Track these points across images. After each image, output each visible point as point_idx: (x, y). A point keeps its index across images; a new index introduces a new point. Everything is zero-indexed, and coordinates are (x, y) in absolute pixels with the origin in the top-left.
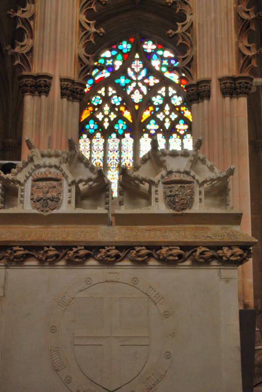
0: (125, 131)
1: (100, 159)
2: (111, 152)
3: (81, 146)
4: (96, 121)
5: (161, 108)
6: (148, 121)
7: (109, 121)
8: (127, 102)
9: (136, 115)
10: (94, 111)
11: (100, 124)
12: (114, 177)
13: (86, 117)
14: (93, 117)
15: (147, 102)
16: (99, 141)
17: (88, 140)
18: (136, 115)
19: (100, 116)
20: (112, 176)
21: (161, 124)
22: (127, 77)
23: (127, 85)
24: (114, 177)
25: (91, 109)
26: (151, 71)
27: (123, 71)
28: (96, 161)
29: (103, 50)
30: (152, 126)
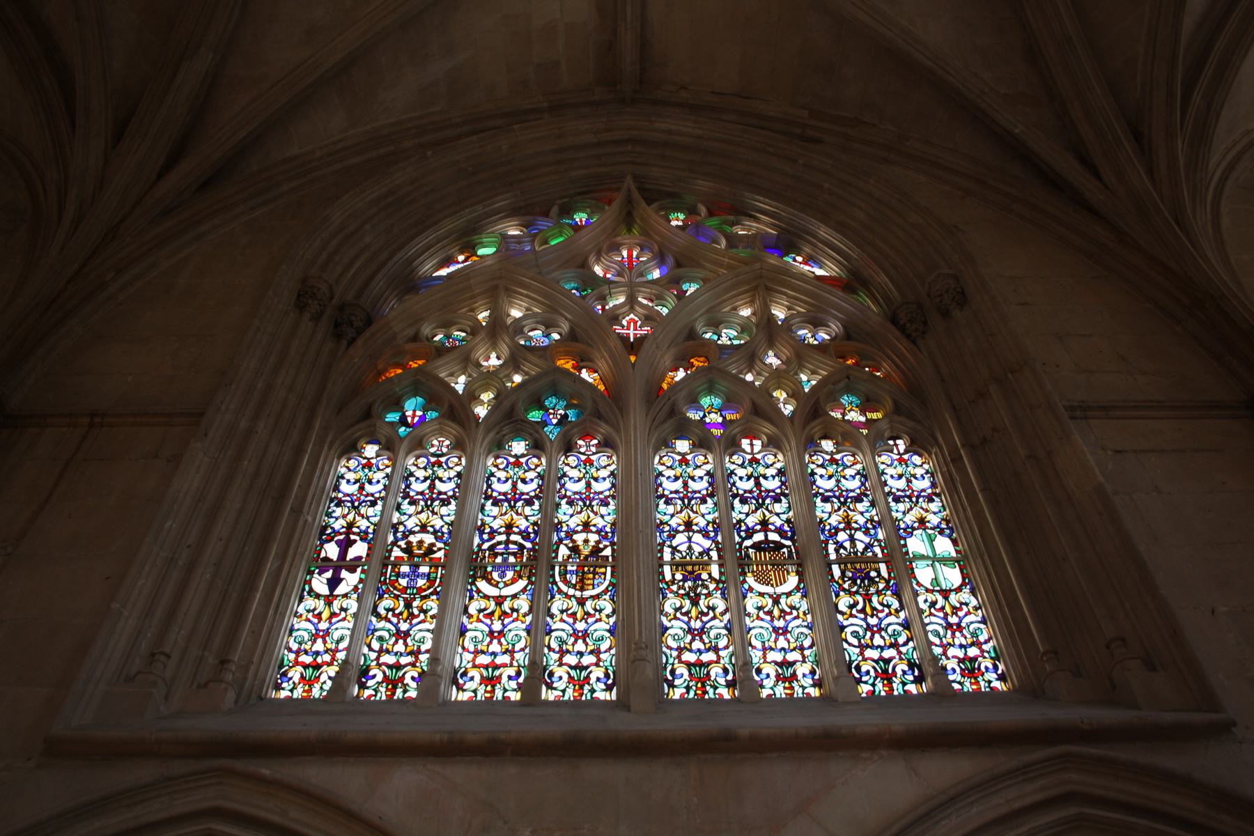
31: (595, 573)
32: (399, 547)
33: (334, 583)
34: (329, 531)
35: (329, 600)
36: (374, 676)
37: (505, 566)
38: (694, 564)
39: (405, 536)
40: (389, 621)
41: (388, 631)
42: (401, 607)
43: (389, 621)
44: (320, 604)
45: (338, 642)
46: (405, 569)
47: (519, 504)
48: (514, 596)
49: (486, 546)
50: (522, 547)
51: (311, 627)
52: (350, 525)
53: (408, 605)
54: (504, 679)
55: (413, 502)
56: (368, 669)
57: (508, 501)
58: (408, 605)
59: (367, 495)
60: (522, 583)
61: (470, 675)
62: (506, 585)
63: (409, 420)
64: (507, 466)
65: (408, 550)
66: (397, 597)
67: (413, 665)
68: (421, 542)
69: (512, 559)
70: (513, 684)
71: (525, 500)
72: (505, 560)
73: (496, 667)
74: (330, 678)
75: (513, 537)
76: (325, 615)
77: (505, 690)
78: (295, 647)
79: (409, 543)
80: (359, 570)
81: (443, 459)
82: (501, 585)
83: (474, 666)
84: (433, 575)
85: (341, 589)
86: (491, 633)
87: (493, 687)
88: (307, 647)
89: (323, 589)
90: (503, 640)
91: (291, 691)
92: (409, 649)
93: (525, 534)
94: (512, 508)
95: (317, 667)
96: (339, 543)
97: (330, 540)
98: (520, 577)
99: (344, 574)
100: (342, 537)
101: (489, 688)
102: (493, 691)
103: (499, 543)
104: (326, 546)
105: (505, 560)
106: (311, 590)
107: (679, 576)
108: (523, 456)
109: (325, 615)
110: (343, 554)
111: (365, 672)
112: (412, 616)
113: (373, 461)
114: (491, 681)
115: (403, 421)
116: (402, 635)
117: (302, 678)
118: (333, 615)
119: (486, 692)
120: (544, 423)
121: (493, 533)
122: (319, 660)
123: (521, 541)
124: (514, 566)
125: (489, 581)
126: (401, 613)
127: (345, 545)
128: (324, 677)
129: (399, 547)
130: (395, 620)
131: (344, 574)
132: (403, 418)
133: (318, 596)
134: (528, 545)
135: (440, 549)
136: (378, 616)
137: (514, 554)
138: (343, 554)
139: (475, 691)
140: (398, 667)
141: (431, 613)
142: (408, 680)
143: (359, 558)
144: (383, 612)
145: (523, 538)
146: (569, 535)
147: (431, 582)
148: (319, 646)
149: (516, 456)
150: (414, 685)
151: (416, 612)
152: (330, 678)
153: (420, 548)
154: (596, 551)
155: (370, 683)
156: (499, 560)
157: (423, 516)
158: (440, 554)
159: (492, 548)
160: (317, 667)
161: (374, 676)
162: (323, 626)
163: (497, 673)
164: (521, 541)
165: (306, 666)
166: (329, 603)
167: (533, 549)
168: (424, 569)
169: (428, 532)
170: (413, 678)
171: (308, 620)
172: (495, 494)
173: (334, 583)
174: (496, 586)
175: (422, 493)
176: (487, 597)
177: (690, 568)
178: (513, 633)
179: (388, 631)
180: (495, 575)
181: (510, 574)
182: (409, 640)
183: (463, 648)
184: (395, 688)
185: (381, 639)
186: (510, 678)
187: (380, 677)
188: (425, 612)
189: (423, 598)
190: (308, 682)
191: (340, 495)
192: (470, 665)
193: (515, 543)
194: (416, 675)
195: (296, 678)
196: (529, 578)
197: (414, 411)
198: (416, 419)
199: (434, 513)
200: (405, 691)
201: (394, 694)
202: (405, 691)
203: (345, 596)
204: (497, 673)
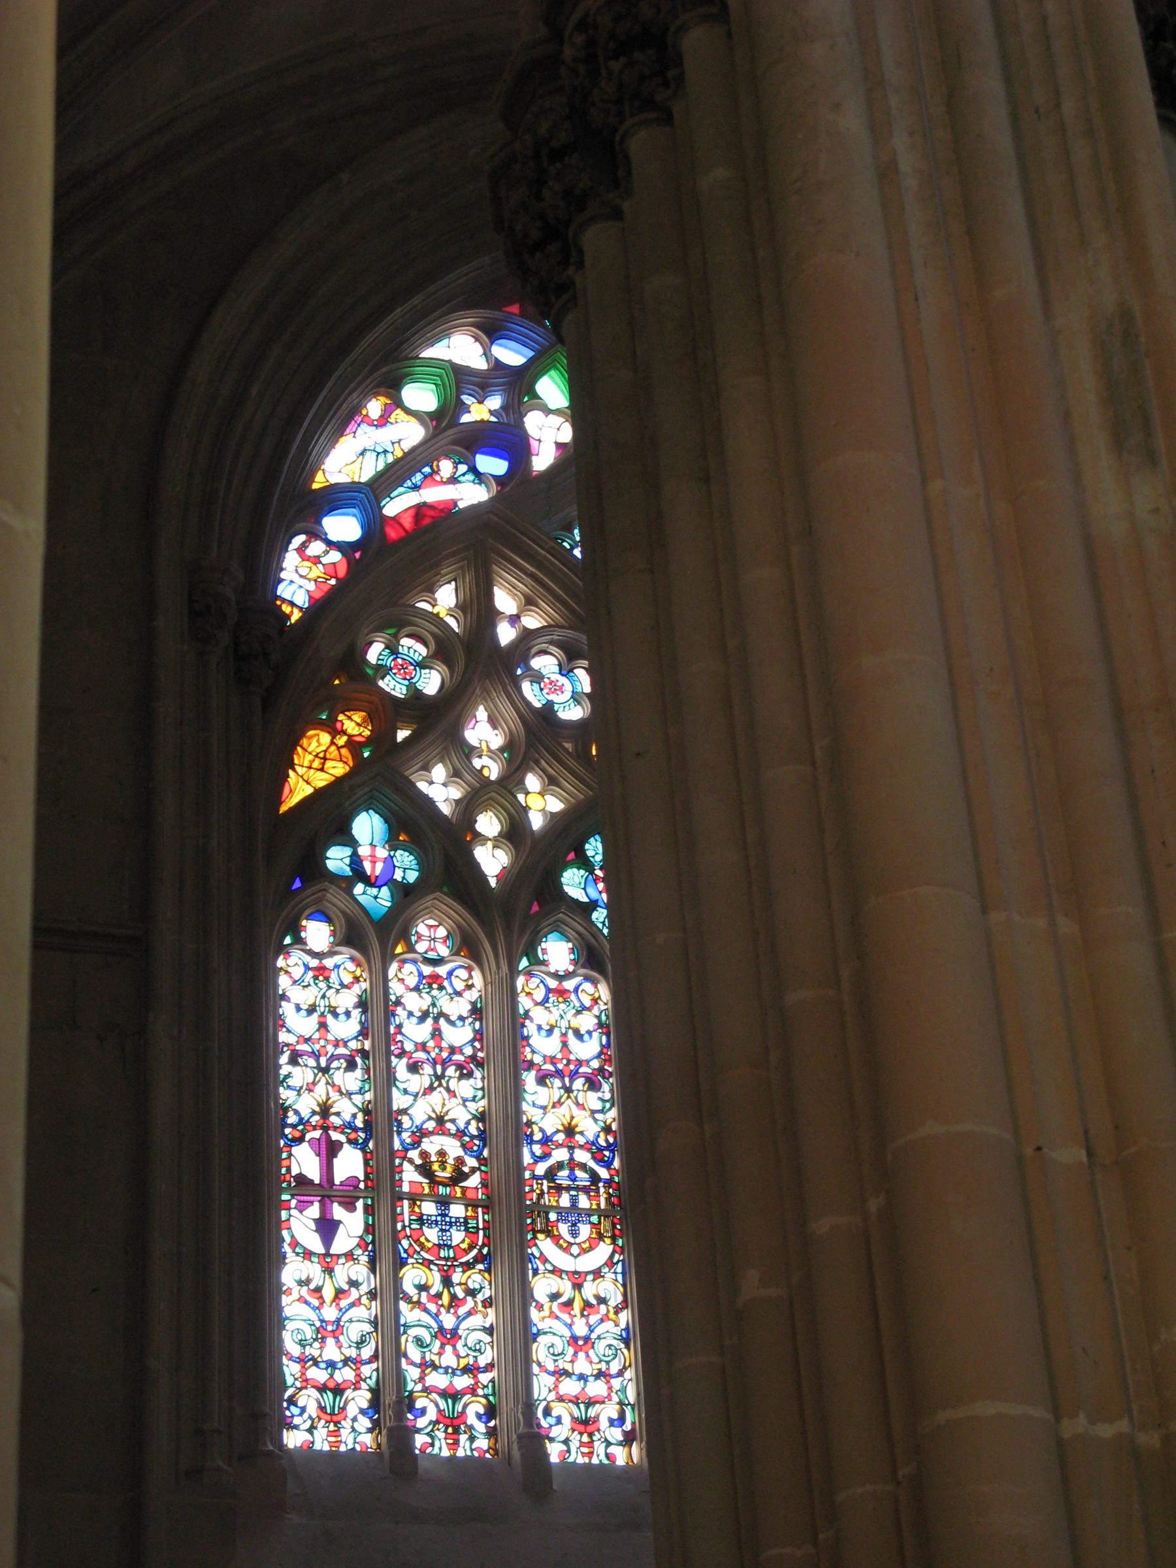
1: (460, 1134)
2: (542, 1080)
3: (287, 1009)
7: (515, 831)
10: (381, 738)
11: (441, 846)
12: (590, 1289)
13: (321, 780)
14: (378, 777)
16: (437, 992)
17: (344, 964)
19: (440, 789)
20: (565, 1287)
24: (590, 1289)
25: (353, 724)
28: (431, 1145)
29: (434, 321)
32: (411, 1161)
33: (327, 1228)
34: (292, 1119)
35: (328, 1264)
36: (423, 1411)
37: (573, 1214)
39: (416, 1143)
40: (426, 1310)
41: (428, 1327)
42: (435, 1279)
43: (426, 1310)
44: (313, 1270)
45: (360, 1344)
46: (429, 1208)
47: (579, 1083)
48: (597, 1274)
49: (541, 1169)
50: (595, 1178)
51: (312, 1316)
52: (325, 1110)
53: (447, 1282)
54: (604, 1423)
55: (414, 1068)
56: (411, 1399)
57: (559, 1074)
58: (447, 1282)
59: (336, 1044)
60: (604, 1250)
61: (555, 1413)
62: (584, 1251)
63: (367, 866)
64: (546, 1000)
65: (425, 1169)
66: (427, 1263)
67: (472, 1391)
68: (442, 1154)
69: (584, 1202)
70: (616, 1434)
71: (585, 1075)
72: (574, 1201)
73: (590, 1403)
74: (363, 1412)
75: (582, 1156)
76: (328, 1293)
77: (609, 1444)
78: (295, 1351)
79: (424, 1155)
80: (360, 1204)
81: (442, 971)
82: (575, 1250)
83: (561, 1399)
84: (472, 1223)
85: (343, 1242)
86: (574, 1339)
87: (591, 1435)
88: (316, 1353)
89: (314, 1243)
90: (591, 1352)
91: (311, 1430)
92: (463, 1362)
94: (568, 1090)
95: (338, 1391)
96: (315, 1145)
97: (300, 1140)
98: (601, 1237)
99: (338, 1212)
100: (317, 1134)
101: (585, 1438)
102: (590, 1444)
103: (560, 1166)
104: (295, 1150)
105: (574, 1201)
106: (295, 1244)
108: (568, 975)
109: (328, 1293)
110: (328, 1169)
111: (407, 1403)
112: (455, 1302)
113: (329, 963)
114: (585, 1425)
116: (448, 1337)
117: (322, 1409)
118: (339, 1293)
119: (582, 1444)
121: (546, 1141)
122: (339, 1377)
123: (592, 1164)
124: (589, 1213)
125: (556, 1239)
126: (439, 1296)
127: (329, 1151)
128: (352, 1410)
129: (411, 1161)
130: (432, 1307)
131: (338, 1212)
133: (308, 1254)
134: (604, 1173)
135: (473, 1170)
136: (408, 1299)
137: (586, 1190)
138: (328, 1169)
139: (566, 1442)
140: (452, 1395)
141: (480, 1297)
142: (471, 1419)
143: (352, 1182)
144: (412, 1291)
145: (594, 1158)
147: (471, 1232)
148: (331, 1352)
149: (555, 975)
150: (480, 1427)
151: (461, 1295)
152: (363, 1412)
153: (444, 1169)
155: (421, 1423)
156: (565, 1200)
157: (437, 1097)
158: (474, 1181)
159: (551, 1174)
160: (338, 1391)
161: (423, 1411)
162: (330, 1313)
163: (592, 1412)
164: (592, 1164)
165: (322, 1389)
166: (329, 1270)
167: (609, 1183)
168: (457, 1211)
169: (447, 1133)
170: (479, 1416)
171: (301, 1299)
172: (537, 1059)
173: (327, 1228)
174: (567, 1250)
175: (422, 1047)
176: (557, 1271)
178: (604, 1343)
179: (428, 1327)
180: (563, 1229)
181: (585, 1231)
182: (459, 1345)
183: (539, 1364)
184: (456, 1431)
185: (419, 1342)
186: (612, 1422)
187: (432, 1414)
188: (472, 1293)
189: (467, 1266)
190: (334, 1417)
191: (291, 1039)
192: (552, 1396)
193: (583, 1167)
194: (482, 1411)
195: (312, 1410)
196: (614, 1242)
197: (373, 846)
198: (379, 867)
199: (452, 1094)
200: (472, 1439)
201: (456, 1443)
202: (472, 1439)
203: (349, 1256)
204: (592, 1412)
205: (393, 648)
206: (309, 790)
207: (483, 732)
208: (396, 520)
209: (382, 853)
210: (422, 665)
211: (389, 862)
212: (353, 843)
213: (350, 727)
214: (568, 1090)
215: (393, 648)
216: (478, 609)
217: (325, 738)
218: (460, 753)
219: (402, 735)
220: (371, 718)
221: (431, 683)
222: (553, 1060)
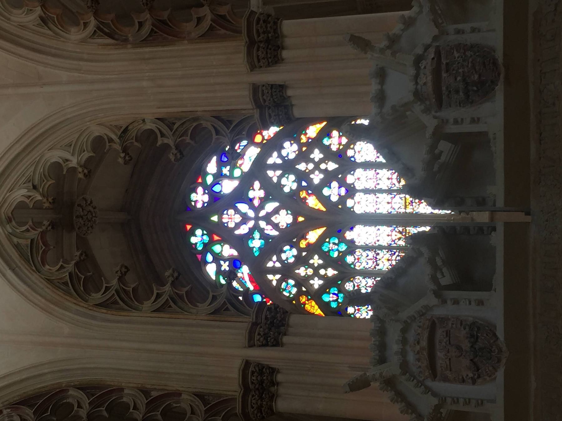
0: (342, 240)
4: (324, 289)
5: (302, 176)
6: (325, 200)
7: (325, 266)
8: (292, 235)
9: (314, 219)
14: (316, 296)
15: (292, 202)
18: (314, 219)
19: (317, 283)
21: (329, 177)
22: (250, 235)
23: (264, 236)
25: (303, 299)
26: (240, 195)
27: (241, 243)
30: (333, 192)
31: (409, 233)
38: (406, 202)
47: (377, 257)
57: (376, 261)
81: (356, 284)
93: (392, 255)
94: (380, 259)
107: (411, 207)
115: (337, 300)
120: (338, 250)
132: (334, 301)
134: (397, 254)
146: (394, 241)
149: (355, 260)
154: (400, 232)
167: (399, 252)
172: (373, 266)
177: (407, 204)
205: (284, 290)
206: (319, 310)
207: (302, 271)
208: (254, 287)
209: (331, 295)
210: (288, 284)
211: (334, 294)
212: (330, 302)
213: (304, 300)
214: (380, 259)
215: (284, 290)
216: (274, 271)
217: (307, 306)
218: (308, 278)
219: (304, 289)
220: (301, 295)
221: (291, 282)
222: (373, 262)
